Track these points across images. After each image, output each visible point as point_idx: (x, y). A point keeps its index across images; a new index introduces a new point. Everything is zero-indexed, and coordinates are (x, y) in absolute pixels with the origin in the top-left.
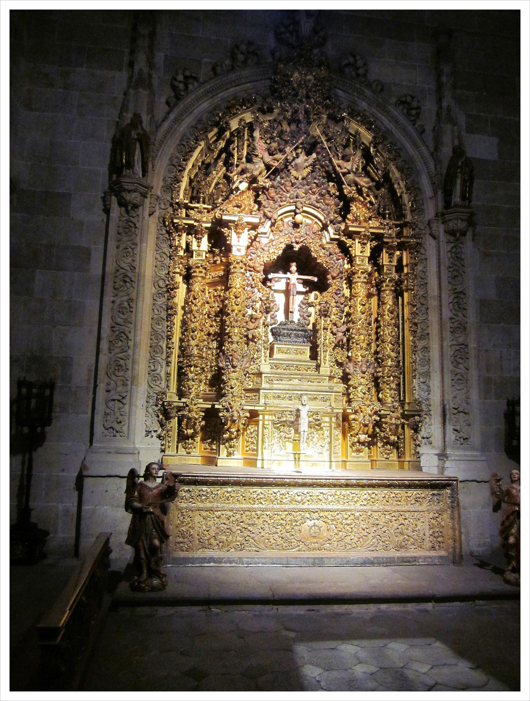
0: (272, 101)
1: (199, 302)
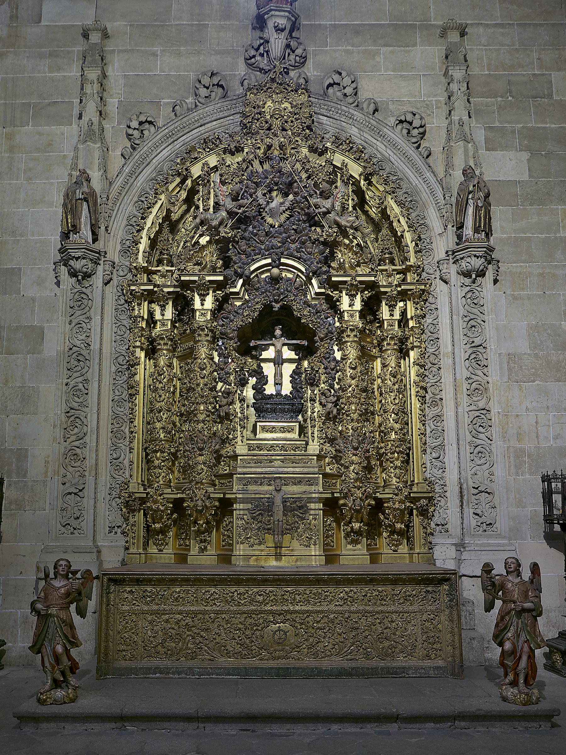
0: (241, 139)
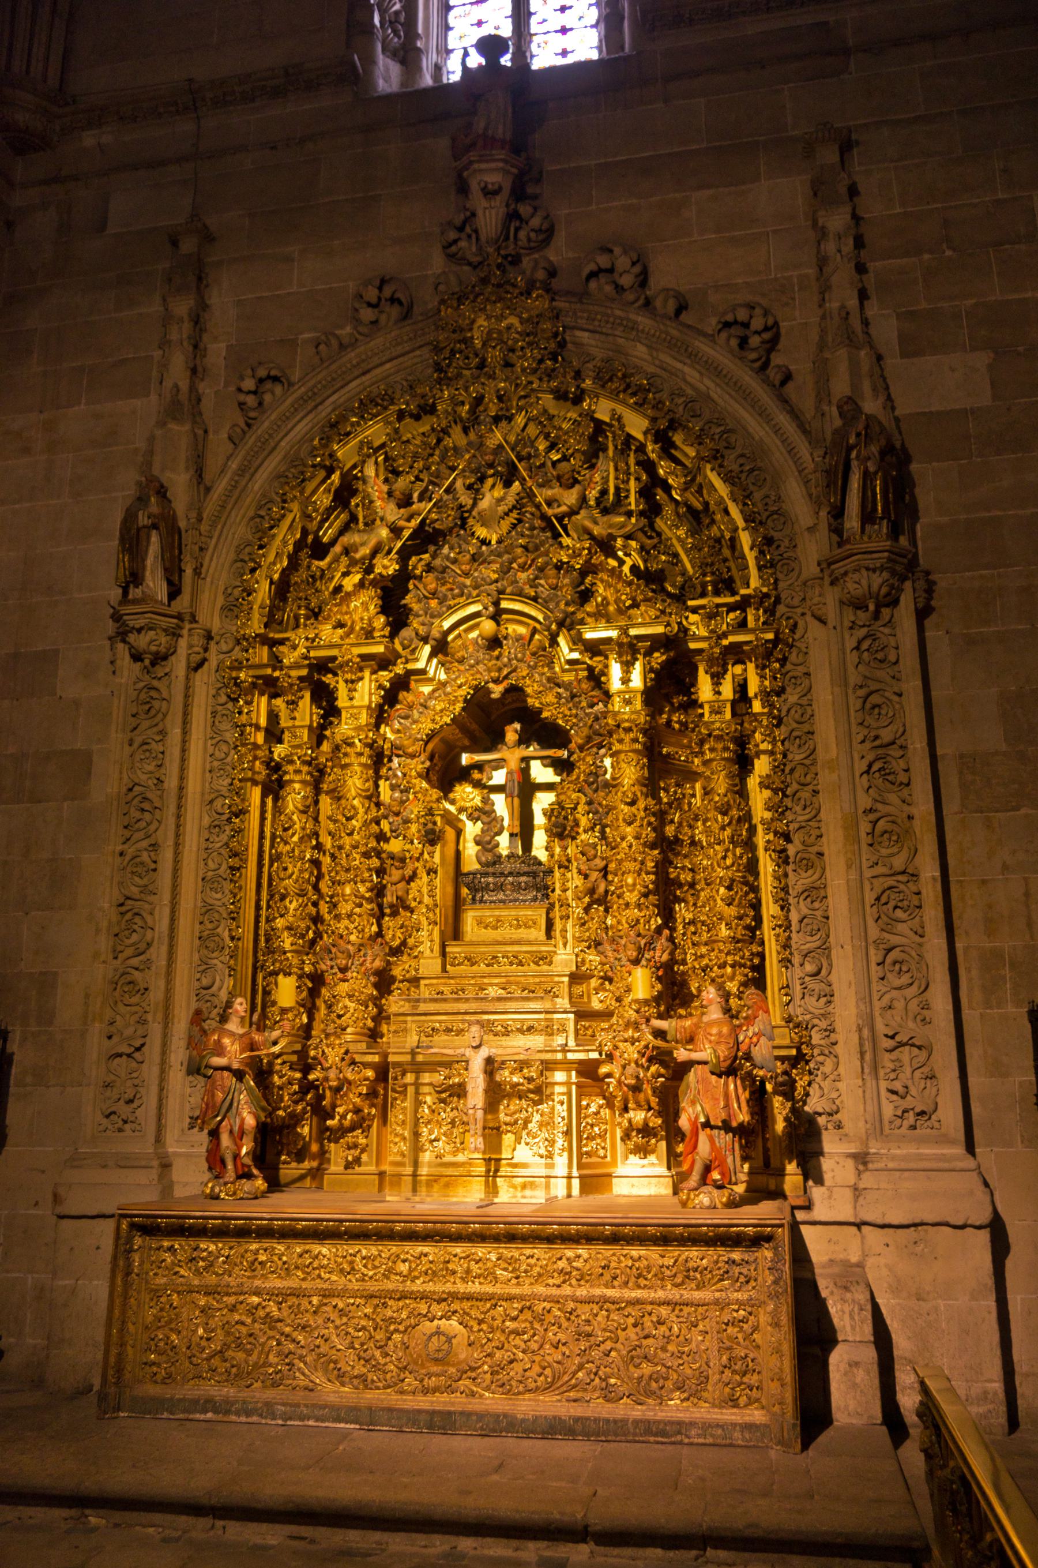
1: (293, 834)
